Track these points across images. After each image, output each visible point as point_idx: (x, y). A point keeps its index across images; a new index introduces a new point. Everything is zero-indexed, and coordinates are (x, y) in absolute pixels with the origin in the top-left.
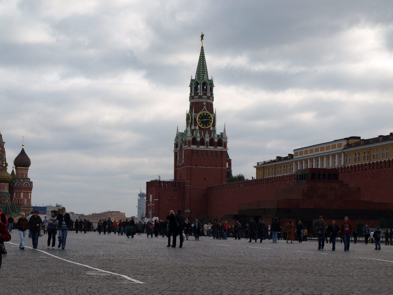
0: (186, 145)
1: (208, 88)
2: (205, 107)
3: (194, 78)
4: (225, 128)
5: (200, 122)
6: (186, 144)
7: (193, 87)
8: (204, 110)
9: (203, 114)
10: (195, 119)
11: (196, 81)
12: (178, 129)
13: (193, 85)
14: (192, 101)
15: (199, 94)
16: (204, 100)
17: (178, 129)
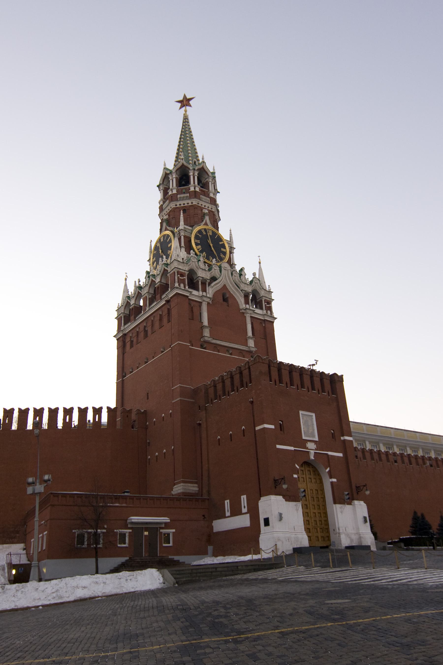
1: (210, 183)
2: (207, 218)
3: (171, 166)
4: (260, 269)
5: (200, 247)
7: (174, 176)
8: (206, 224)
9: (205, 230)
15: (192, 189)
16: (204, 203)
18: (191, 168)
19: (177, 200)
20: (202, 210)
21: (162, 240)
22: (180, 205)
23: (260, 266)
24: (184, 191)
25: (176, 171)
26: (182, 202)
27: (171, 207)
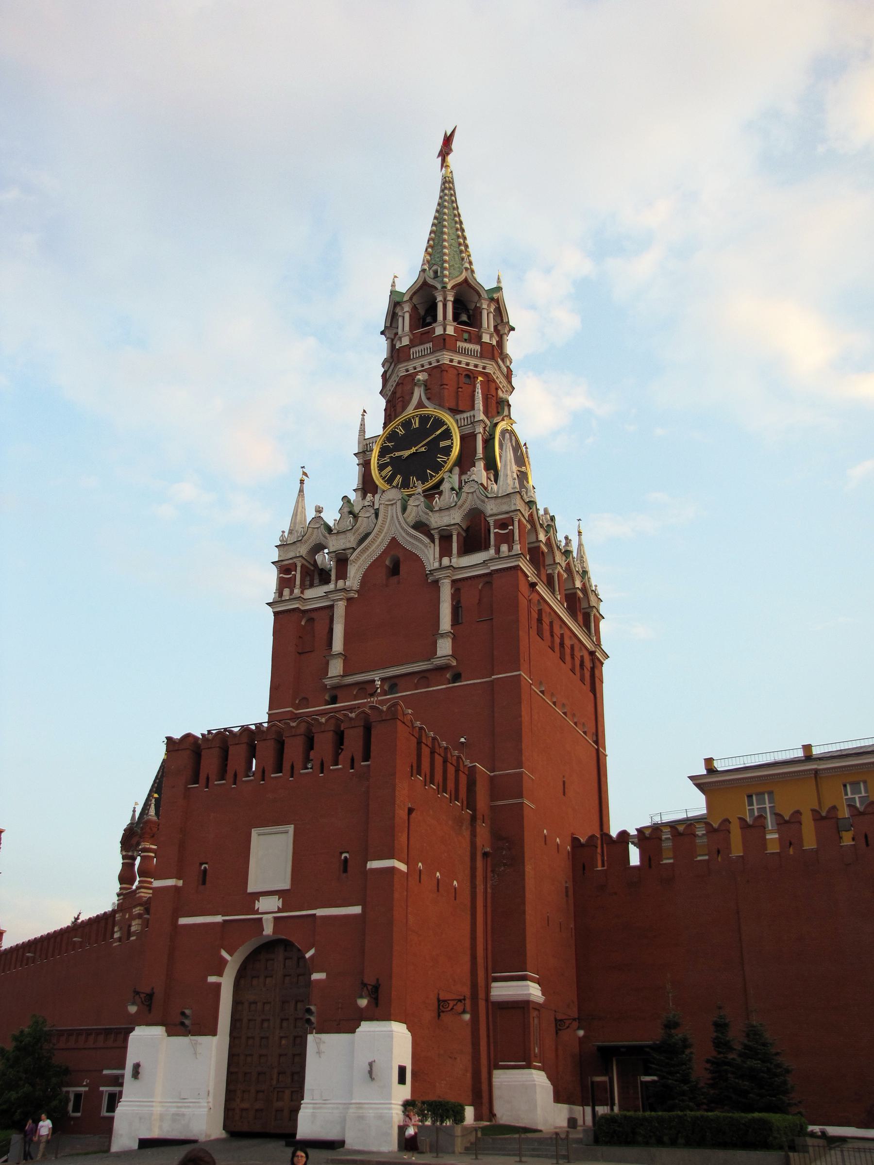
0: (508, 539)
4: (580, 545)
6: (467, 548)
7: (450, 298)
10: (489, 442)
11: (466, 281)
12: (301, 491)
13: (449, 287)
14: (446, 357)
15: (486, 338)
17: (301, 491)
18: (484, 295)
19: (455, 350)
20: (497, 389)
21: (416, 424)
22: (460, 362)
23: (580, 539)
24: (466, 336)
25: (453, 288)
26: (464, 360)
27: (438, 361)
